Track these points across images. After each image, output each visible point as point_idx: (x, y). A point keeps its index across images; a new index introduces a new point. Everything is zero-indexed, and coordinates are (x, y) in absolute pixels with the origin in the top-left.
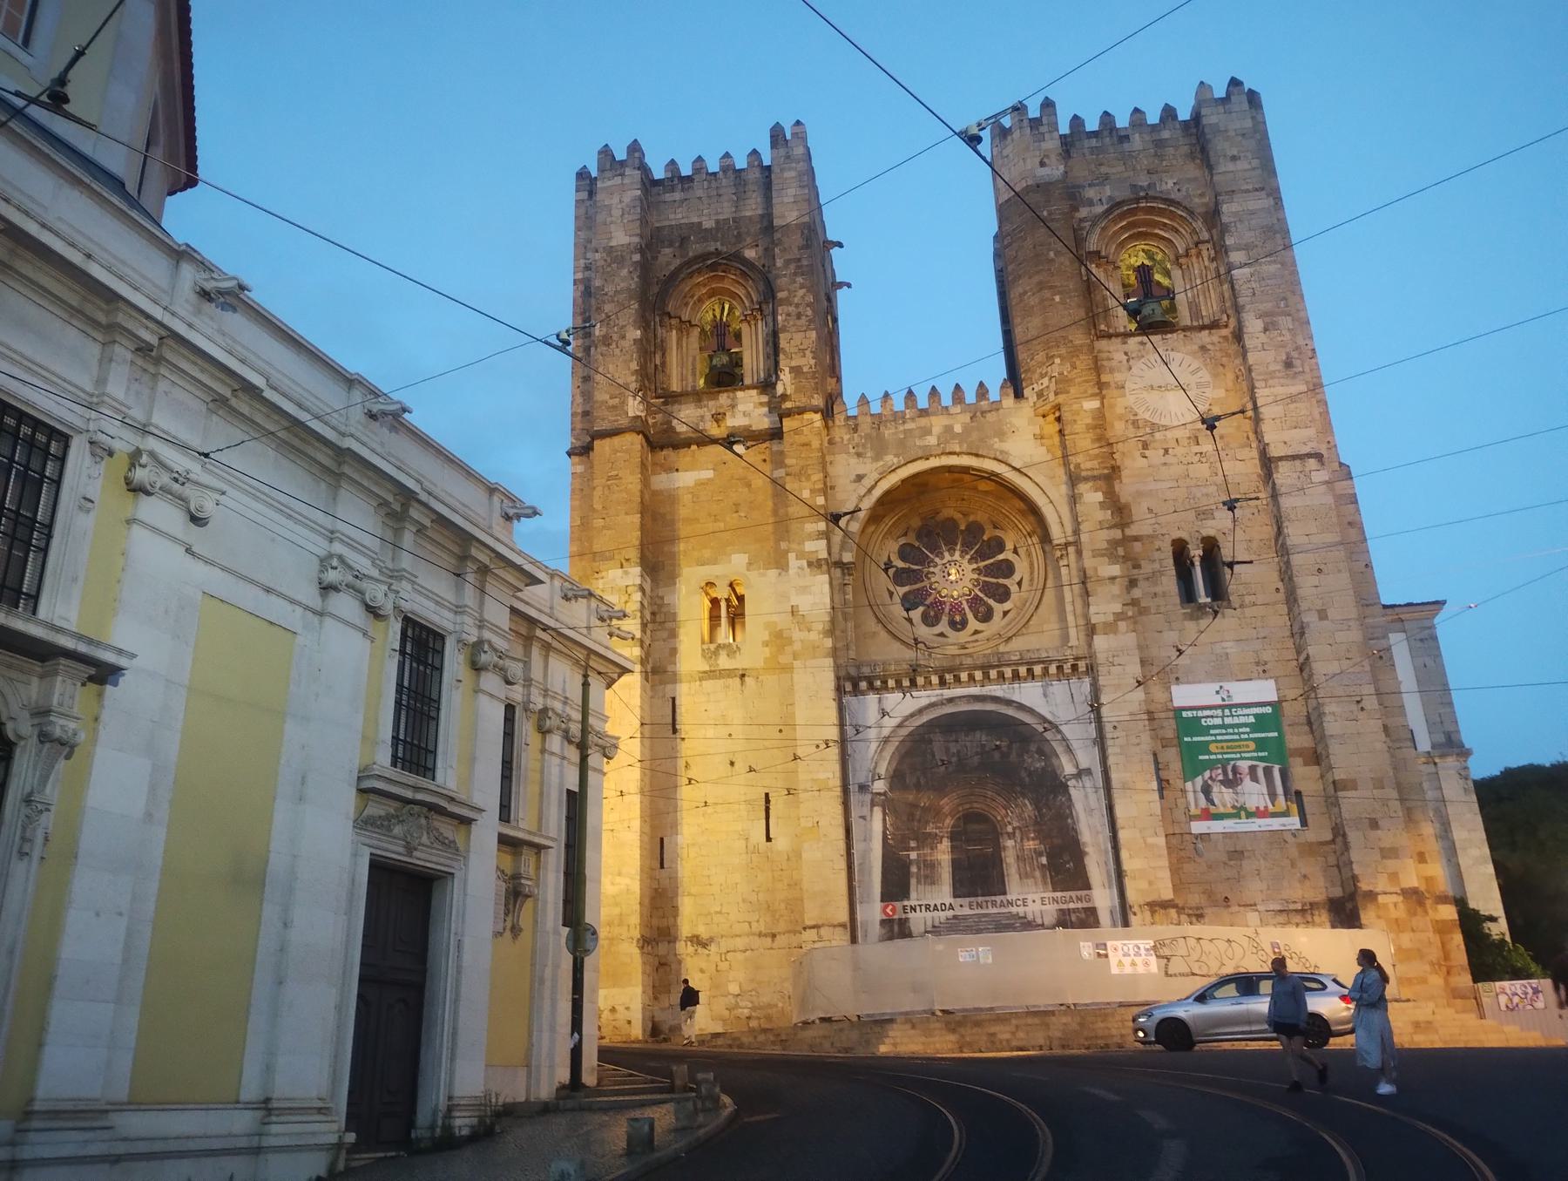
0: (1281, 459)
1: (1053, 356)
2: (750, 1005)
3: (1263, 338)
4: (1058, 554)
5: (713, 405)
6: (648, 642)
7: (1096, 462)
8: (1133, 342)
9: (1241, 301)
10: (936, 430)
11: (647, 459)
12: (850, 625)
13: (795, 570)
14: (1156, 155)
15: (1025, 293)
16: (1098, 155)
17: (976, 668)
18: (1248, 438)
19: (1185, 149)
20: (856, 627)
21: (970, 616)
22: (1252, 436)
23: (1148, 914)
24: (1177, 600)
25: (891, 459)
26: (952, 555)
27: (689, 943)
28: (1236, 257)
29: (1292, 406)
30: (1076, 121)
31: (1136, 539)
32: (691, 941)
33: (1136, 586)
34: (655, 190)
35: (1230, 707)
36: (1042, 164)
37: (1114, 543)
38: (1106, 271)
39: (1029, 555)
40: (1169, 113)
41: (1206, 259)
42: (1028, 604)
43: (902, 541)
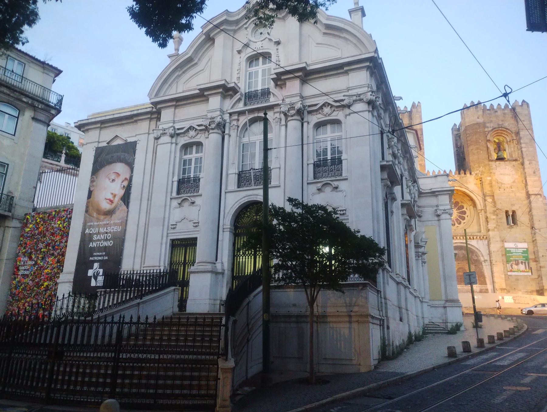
3: (529, 166)
9: (524, 156)
14: (504, 117)
19: (511, 116)
22: (524, 188)
23: (500, 291)
28: (523, 145)
35: (517, 248)
36: (478, 118)
39: (470, 210)
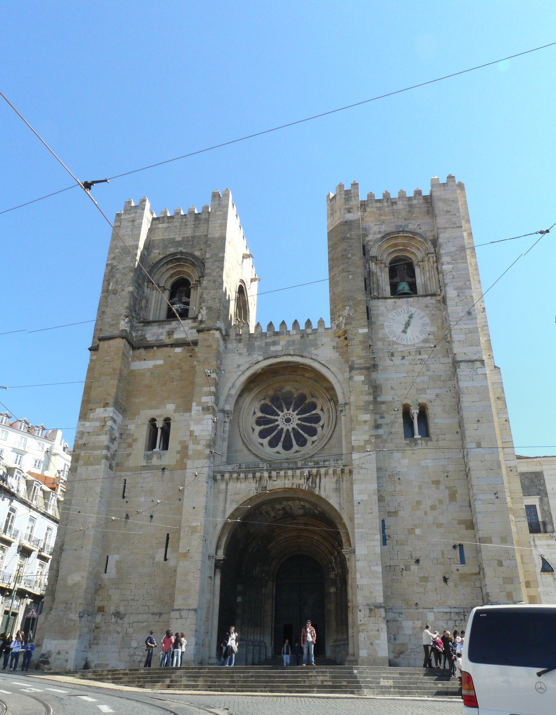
0: (461, 361)
1: (344, 306)
2: (141, 654)
3: (457, 300)
4: (340, 409)
5: (168, 327)
6: (114, 447)
7: (363, 360)
8: (389, 301)
9: (446, 281)
10: (283, 343)
11: (128, 353)
12: (226, 444)
13: (195, 412)
15: (335, 275)
16: (380, 211)
17: (288, 469)
18: (447, 351)
20: (229, 447)
21: (294, 443)
24: (403, 436)
25: (257, 356)
26: (288, 410)
27: (113, 616)
28: (445, 259)
29: (470, 335)
30: (371, 196)
31: (383, 403)
32: (115, 616)
33: (381, 427)
34: (154, 222)
36: (349, 212)
37: (368, 403)
38: (380, 268)
40: (418, 193)
41: (431, 262)
42: (325, 437)
43: (263, 402)
